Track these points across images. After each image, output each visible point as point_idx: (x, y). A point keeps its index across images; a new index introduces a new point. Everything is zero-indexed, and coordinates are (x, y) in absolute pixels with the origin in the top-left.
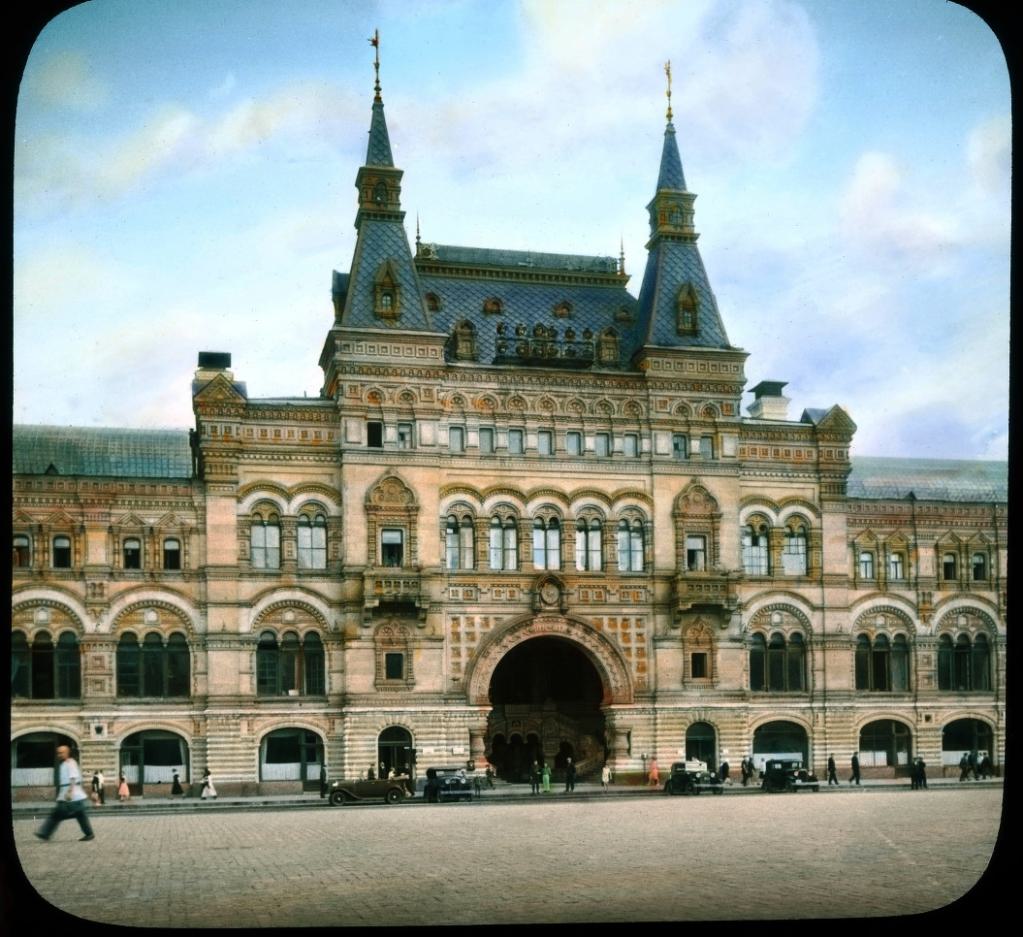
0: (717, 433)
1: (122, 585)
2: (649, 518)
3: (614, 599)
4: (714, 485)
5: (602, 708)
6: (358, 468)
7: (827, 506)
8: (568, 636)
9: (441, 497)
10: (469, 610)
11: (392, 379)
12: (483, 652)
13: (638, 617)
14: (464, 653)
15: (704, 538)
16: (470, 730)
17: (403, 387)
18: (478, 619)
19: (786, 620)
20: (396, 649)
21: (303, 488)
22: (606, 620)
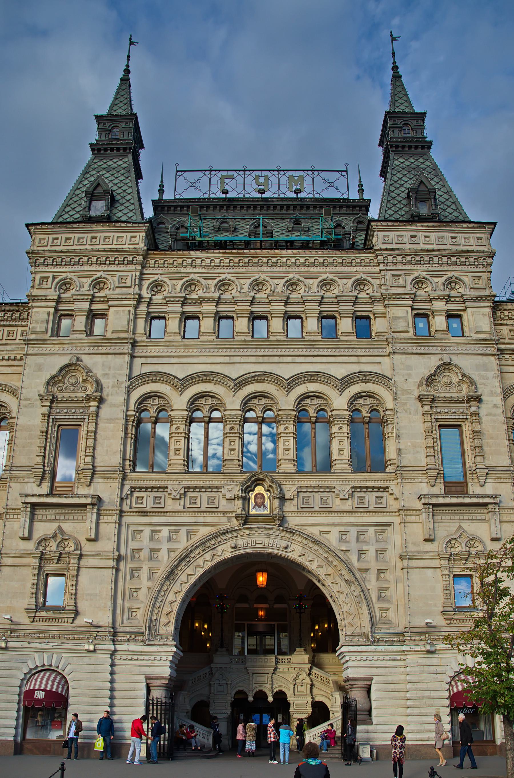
3: (347, 506)
4: (466, 363)
6: (40, 359)
8: (283, 554)
10: (155, 519)
11: (86, 268)
12: (171, 575)
13: (379, 528)
14: (144, 574)
15: (459, 426)
16: (147, 678)
18: (165, 531)
22: (335, 531)
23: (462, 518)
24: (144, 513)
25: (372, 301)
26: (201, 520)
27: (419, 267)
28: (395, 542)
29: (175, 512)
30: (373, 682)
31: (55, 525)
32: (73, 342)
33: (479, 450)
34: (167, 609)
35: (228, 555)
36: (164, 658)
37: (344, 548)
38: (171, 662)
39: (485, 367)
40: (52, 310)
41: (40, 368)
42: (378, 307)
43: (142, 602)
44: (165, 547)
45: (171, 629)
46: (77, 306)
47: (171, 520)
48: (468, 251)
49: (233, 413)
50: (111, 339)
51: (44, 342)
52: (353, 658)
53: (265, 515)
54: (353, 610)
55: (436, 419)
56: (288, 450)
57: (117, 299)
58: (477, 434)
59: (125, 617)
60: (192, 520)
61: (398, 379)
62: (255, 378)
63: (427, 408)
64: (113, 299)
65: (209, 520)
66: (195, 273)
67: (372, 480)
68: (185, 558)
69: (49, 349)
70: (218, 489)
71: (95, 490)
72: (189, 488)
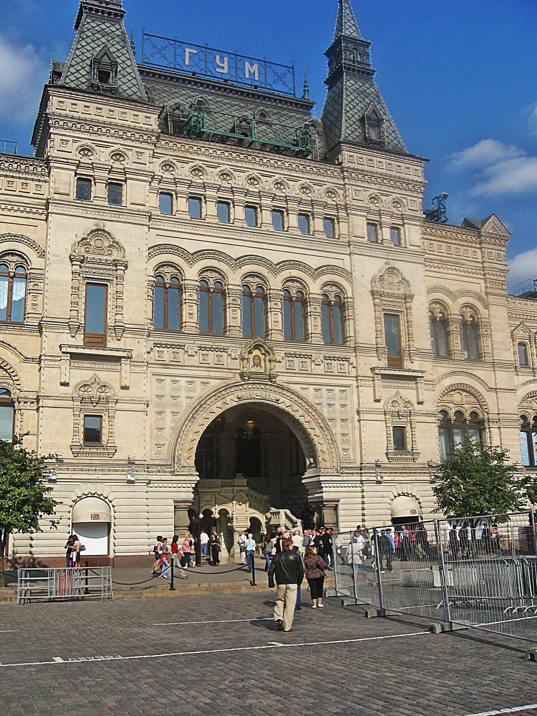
0: (403, 225)
2: (350, 295)
3: (320, 369)
5: (303, 481)
9: (150, 256)
11: (104, 139)
16: (175, 502)
17: (116, 147)
19: (465, 400)
23: (399, 385)
24: (166, 366)
25: (337, 207)
26: (213, 374)
27: (373, 186)
29: (192, 366)
30: (340, 502)
31: (91, 373)
32: (96, 208)
34: (188, 446)
35: (235, 404)
36: (189, 485)
37: (317, 402)
38: (193, 488)
40: (73, 173)
42: (342, 214)
43: (167, 440)
44: (183, 394)
45: (192, 462)
46: (97, 173)
47: (188, 373)
48: (408, 180)
49: (236, 288)
50: (131, 210)
51: (69, 204)
52: (327, 485)
53: (261, 373)
54: (325, 449)
55: (383, 309)
56: (277, 322)
57: (134, 174)
59: (153, 452)
60: (205, 374)
62: (13, 238)
63: (377, 301)
64: (130, 173)
65: (219, 374)
66: (200, 160)
68: (201, 405)
69: (73, 210)
70: (224, 350)
71: (125, 344)
72: (201, 347)
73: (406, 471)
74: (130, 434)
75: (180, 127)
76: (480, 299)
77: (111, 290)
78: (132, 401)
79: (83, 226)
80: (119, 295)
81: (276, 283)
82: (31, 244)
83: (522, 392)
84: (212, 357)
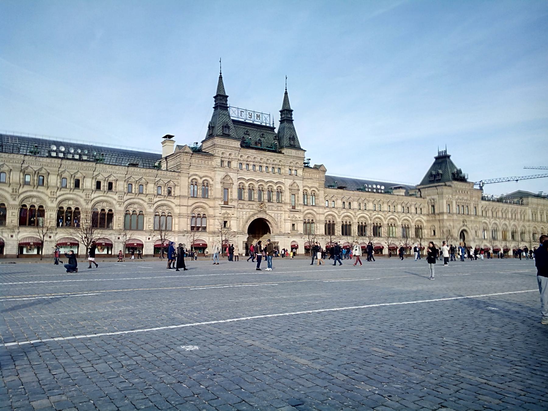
1: (157, 199)
3: (276, 209)
4: (297, 181)
7: (320, 189)
20: (226, 220)
21: (204, 177)
25: (282, 165)
28: (283, 217)
33: (298, 200)
39: (300, 183)
41: (219, 174)
42: (283, 167)
58: (298, 197)
61: (286, 184)
67: (280, 205)
73: (295, 235)
74: (234, 225)
75: (245, 145)
76: (317, 189)
77: (229, 190)
78: (234, 217)
79: (223, 174)
80: (231, 192)
81: (266, 187)
82: (211, 178)
83: (326, 214)
84: (251, 206)
